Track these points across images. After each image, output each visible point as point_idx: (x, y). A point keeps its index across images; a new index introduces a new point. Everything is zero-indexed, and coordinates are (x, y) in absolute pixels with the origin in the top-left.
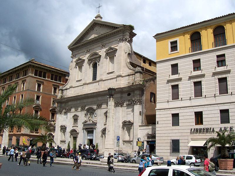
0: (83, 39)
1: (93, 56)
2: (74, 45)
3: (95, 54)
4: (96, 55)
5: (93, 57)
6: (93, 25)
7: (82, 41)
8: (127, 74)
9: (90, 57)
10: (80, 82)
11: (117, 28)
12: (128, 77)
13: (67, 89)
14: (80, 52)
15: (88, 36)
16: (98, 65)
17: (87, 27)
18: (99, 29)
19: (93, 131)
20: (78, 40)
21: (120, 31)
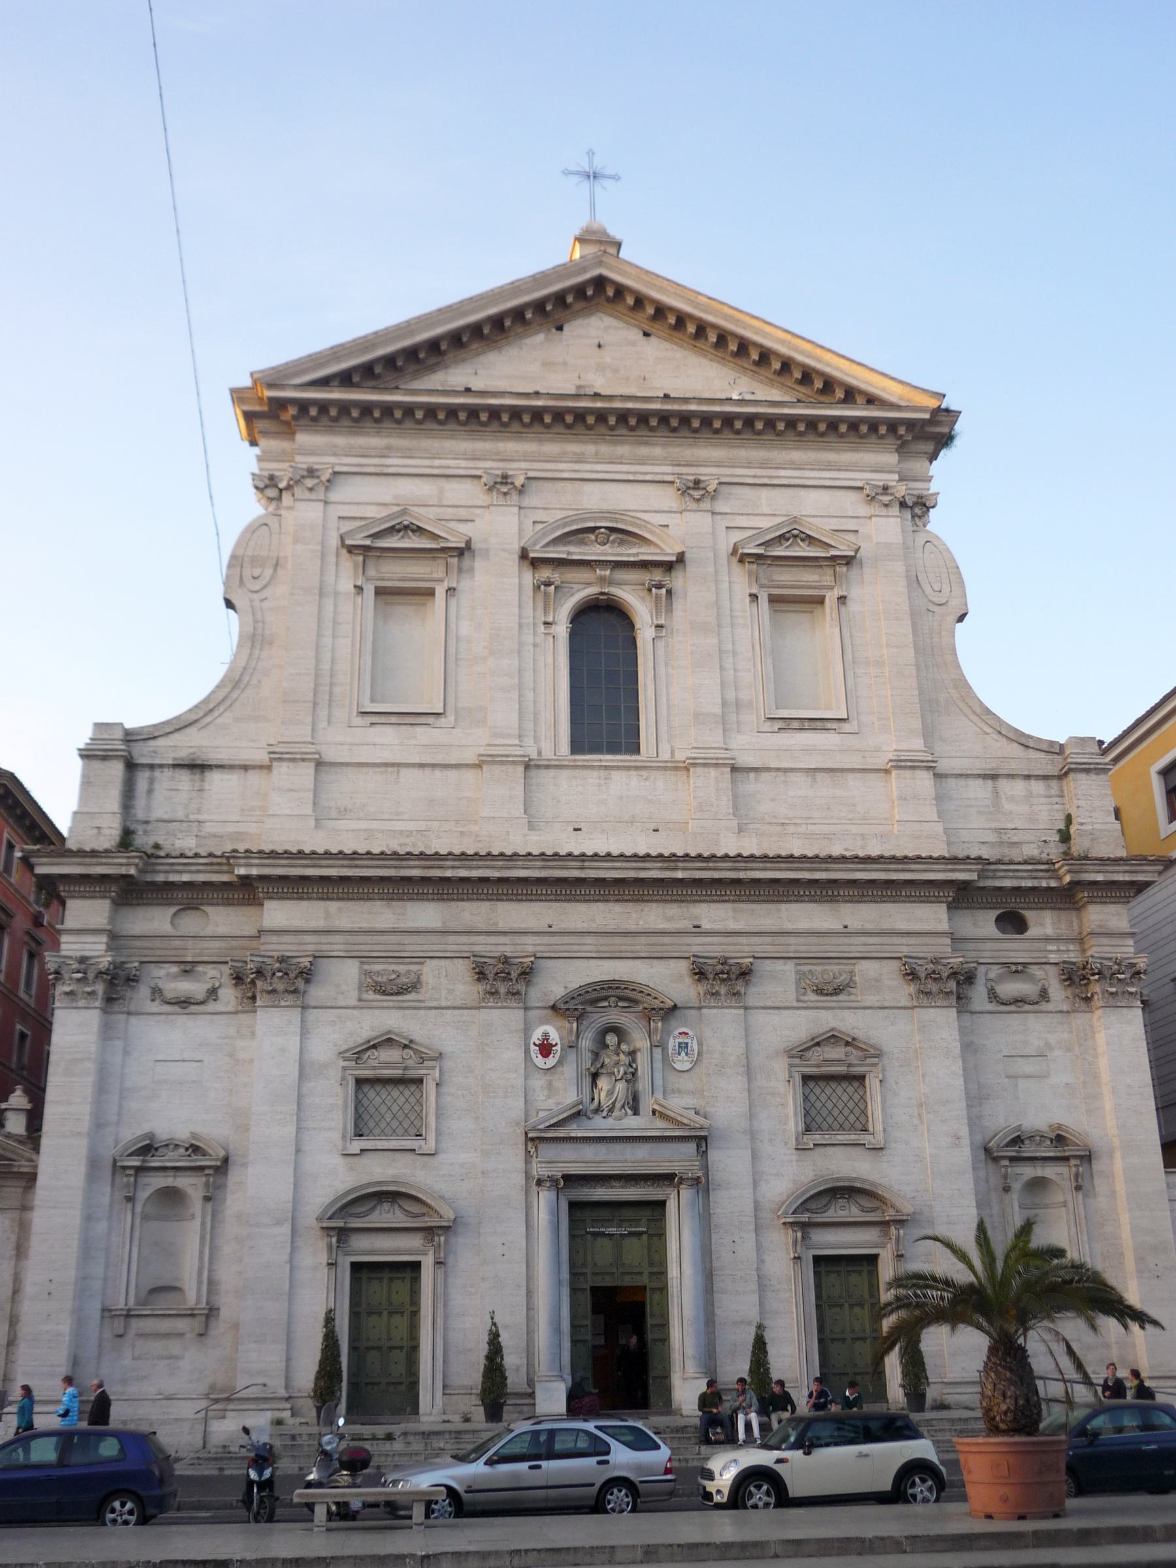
0: (432, 369)
1: (582, 543)
2: (324, 382)
3: (612, 530)
4: (621, 543)
5: (576, 552)
6: (579, 291)
7: (417, 375)
8: (977, 767)
9: (556, 541)
10: (423, 735)
11: (851, 395)
12: (978, 790)
13: (197, 767)
14: (394, 463)
15: (492, 357)
16: (645, 634)
17: (515, 288)
18: (633, 344)
19: (662, 1204)
20: (390, 361)
21: (893, 425)
